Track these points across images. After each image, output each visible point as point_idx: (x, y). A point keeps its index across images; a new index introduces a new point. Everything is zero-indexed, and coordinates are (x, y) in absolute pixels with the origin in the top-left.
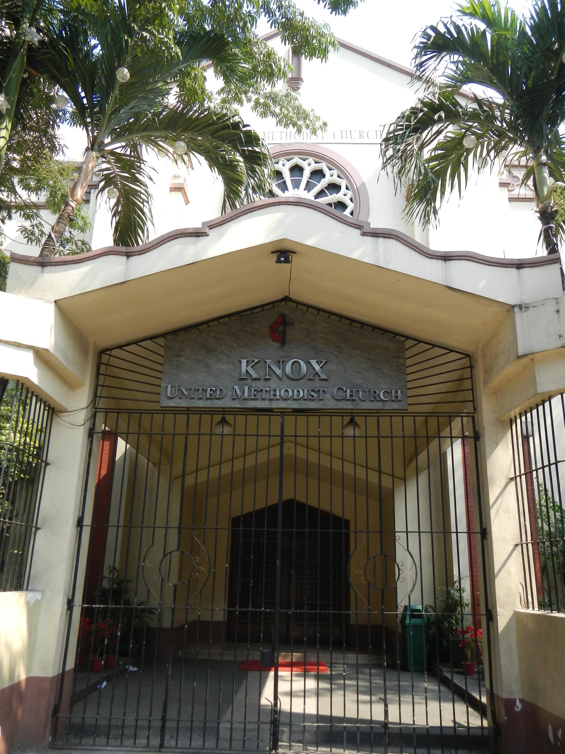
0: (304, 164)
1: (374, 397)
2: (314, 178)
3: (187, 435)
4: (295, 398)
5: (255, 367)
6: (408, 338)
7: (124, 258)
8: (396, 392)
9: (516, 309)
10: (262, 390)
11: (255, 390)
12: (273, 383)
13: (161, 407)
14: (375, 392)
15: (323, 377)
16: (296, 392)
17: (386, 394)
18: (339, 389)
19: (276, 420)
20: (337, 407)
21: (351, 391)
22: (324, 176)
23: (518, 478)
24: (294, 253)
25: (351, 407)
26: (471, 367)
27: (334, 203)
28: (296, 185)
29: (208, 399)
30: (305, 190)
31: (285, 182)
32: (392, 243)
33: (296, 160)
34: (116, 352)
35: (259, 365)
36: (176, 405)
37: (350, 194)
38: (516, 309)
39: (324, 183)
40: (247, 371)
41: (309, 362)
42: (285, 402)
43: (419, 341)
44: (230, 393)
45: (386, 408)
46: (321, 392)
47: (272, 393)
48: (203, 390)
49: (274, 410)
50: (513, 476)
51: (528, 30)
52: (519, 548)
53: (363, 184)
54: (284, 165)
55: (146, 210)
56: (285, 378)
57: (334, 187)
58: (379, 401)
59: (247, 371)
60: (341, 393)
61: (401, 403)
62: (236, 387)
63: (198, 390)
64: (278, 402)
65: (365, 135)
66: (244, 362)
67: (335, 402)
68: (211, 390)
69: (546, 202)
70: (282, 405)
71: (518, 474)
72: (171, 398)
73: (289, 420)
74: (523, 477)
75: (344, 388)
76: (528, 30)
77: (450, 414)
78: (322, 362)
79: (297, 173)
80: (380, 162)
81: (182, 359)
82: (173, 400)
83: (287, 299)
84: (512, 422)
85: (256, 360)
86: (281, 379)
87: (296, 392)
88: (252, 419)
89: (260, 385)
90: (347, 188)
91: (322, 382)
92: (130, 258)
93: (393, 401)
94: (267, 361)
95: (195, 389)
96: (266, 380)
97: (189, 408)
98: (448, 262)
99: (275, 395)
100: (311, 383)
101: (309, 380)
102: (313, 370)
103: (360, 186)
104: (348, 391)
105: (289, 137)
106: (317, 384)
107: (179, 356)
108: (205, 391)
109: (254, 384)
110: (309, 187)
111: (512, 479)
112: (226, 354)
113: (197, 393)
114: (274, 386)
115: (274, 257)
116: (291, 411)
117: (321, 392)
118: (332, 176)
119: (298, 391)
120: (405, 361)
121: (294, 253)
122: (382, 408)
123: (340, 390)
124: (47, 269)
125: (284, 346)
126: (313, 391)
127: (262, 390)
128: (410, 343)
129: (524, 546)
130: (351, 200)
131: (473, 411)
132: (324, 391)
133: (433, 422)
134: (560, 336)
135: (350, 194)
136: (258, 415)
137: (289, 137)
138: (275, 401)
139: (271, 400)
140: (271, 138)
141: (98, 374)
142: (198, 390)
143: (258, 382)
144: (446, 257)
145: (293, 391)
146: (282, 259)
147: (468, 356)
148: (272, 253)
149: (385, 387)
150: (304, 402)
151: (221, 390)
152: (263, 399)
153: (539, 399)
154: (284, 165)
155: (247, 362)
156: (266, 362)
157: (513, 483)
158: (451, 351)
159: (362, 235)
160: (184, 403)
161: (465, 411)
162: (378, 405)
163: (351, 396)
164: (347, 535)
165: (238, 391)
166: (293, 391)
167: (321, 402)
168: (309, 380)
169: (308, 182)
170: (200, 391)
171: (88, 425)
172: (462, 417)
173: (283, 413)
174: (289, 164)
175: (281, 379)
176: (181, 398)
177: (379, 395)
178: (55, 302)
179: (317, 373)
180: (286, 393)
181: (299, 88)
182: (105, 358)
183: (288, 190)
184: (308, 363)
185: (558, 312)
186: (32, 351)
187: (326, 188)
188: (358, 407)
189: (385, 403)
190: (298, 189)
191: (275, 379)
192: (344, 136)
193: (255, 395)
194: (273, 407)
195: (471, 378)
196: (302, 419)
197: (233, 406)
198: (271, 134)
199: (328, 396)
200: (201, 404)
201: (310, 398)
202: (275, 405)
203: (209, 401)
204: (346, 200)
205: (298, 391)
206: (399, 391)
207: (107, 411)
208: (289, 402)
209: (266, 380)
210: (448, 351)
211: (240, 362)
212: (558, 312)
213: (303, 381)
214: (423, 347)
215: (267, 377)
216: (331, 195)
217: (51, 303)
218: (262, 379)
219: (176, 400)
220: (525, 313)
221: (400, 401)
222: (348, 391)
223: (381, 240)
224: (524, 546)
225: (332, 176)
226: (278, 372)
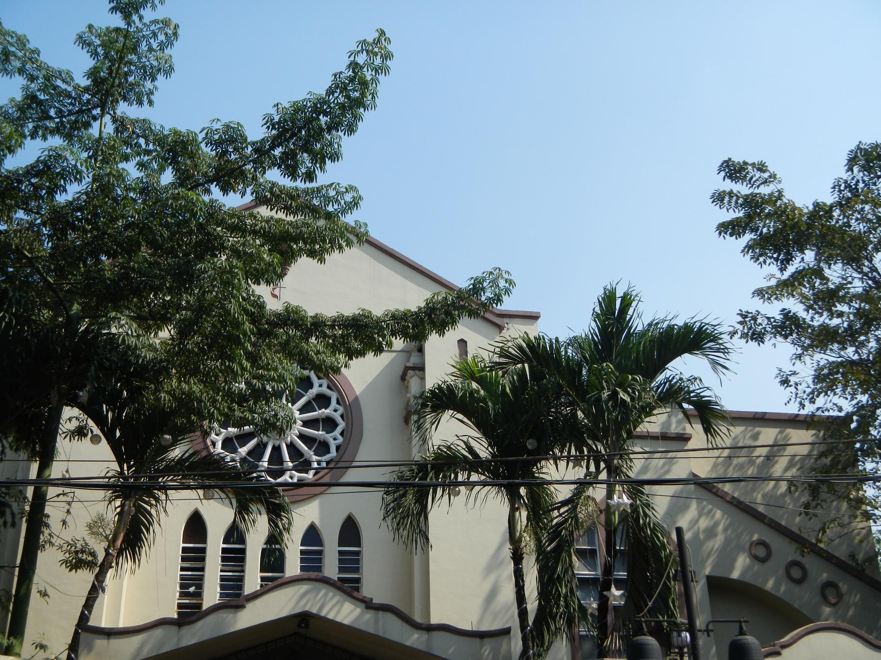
7: (176, 628)
22: (311, 385)
32: (390, 618)
37: (341, 410)
53: (356, 399)
55: (153, 512)
80: (381, 514)
90: (338, 403)
118: (320, 386)
130: (342, 416)
144: (430, 628)
146: (303, 625)
187: (313, 399)
204: (337, 416)
223: (381, 613)
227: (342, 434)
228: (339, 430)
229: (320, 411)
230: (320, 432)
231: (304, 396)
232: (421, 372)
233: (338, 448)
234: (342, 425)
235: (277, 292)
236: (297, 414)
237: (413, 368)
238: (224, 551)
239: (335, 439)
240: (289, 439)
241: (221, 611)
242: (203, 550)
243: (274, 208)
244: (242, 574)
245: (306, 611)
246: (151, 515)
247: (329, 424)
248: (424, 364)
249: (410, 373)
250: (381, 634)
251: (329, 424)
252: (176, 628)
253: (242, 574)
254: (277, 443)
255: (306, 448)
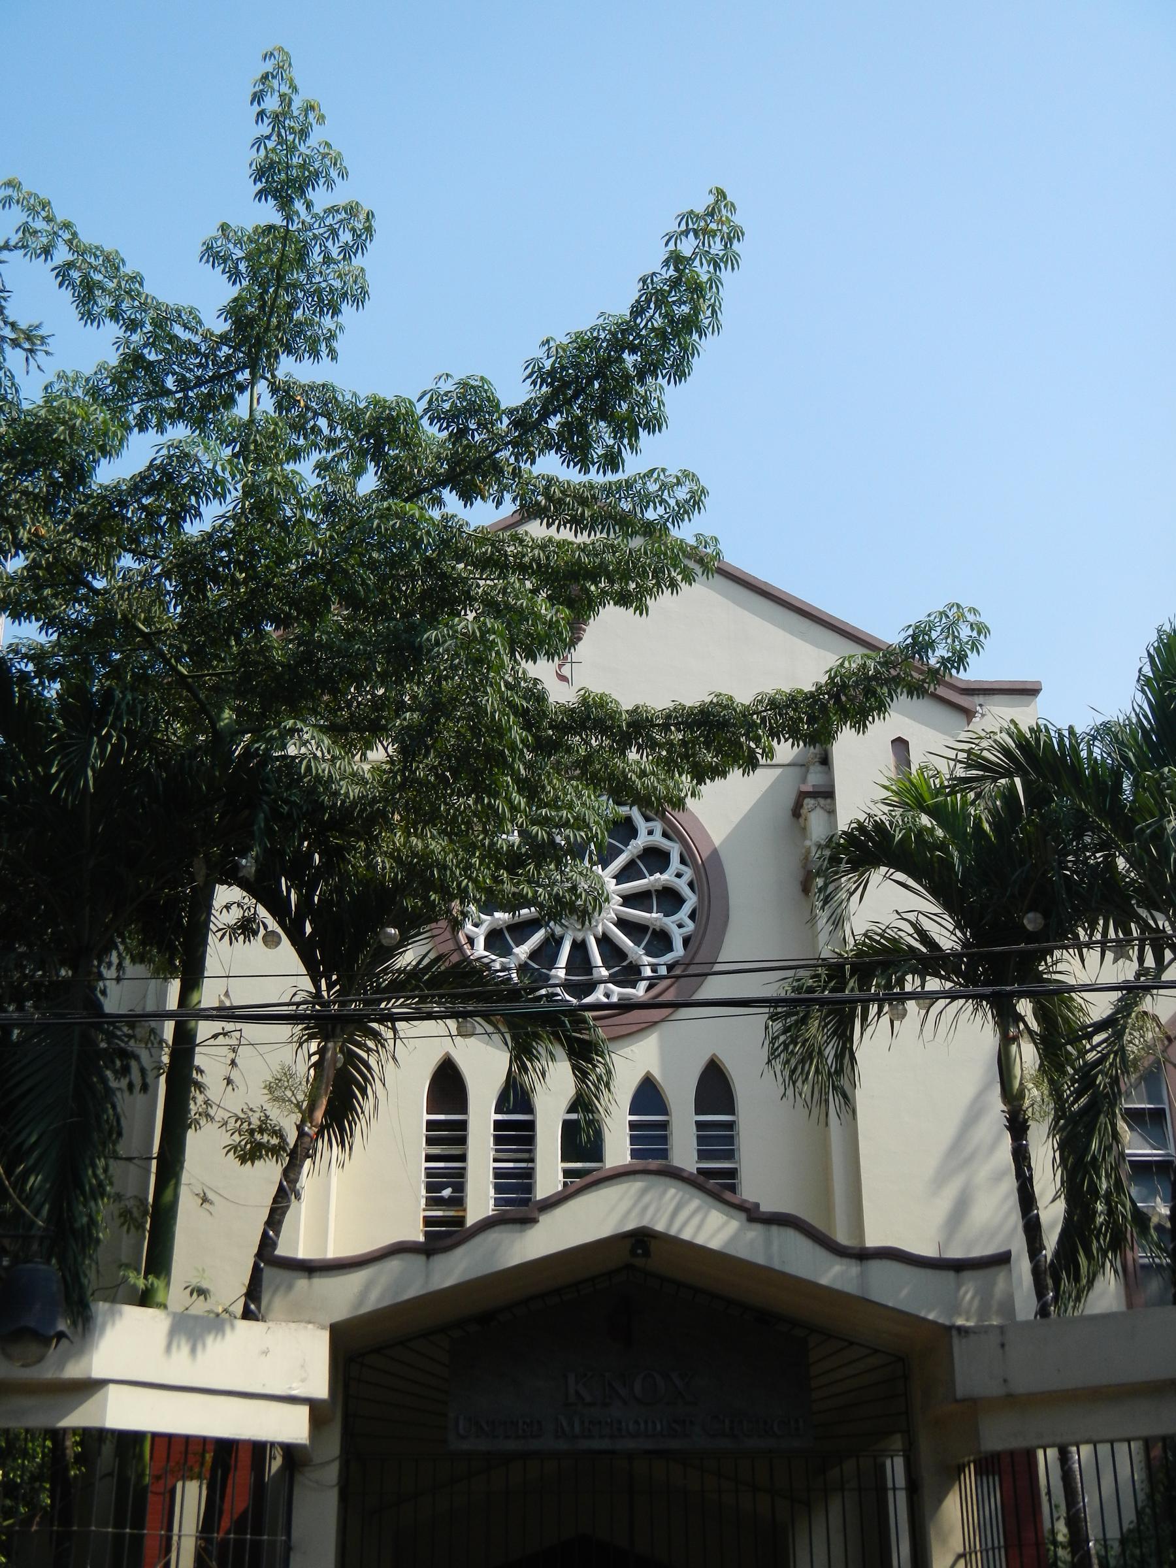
9: (954, 1333)
22: (634, 833)
32: (791, 1235)
37: (688, 873)
38: (954, 1333)
40: (577, 1393)
50: (961, 1550)
51: (986, 826)
53: (715, 853)
55: (372, 1062)
59: (577, 1393)
68: (524, 1423)
69: (1015, 1103)
70: (631, 1444)
76: (986, 826)
80: (764, 1054)
92: (431, 1258)
98: (865, 1262)
103: (708, 858)
118: (650, 833)
124: (315, 1274)
130: (691, 885)
134: (1005, 1381)
144: (863, 1255)
146: (640, 1251)
157: (962, 1561)
165: (565, 1424)
166: (646, 1422)
185: (1003, 1345)
187: (639, 857)
204: (682, 885)
212: (1003, 1345)
217: (323, 1328)
220: (964, 1341)
223: (774, 1229)
225: (650, 833)
227: (692, 916)
228: (687, 909)
229: (652, 878)
230: (654, 915)
231: (622, 851)
232: (829, 801)
233: (686, 941)
234: (691, 900)
235: (566, 671)
236: (611, 885)
237: (814, 795)
238: (498, 1125)
239: (680, 926)
240: (600, 929)
241: (497, 1229)
242: (463, 1125)
243: (553, 523)
244: (530, 1165)
245: (644, 1227)
246: (369, 1068)
247: (670, 899)
248: (833, 786)
249: (809, 803)
250: (777, 1265)
251: (670, 899)
252: (421, 1259)
253: (530, 1165)
254: (580, 936)
255: (631, 944)
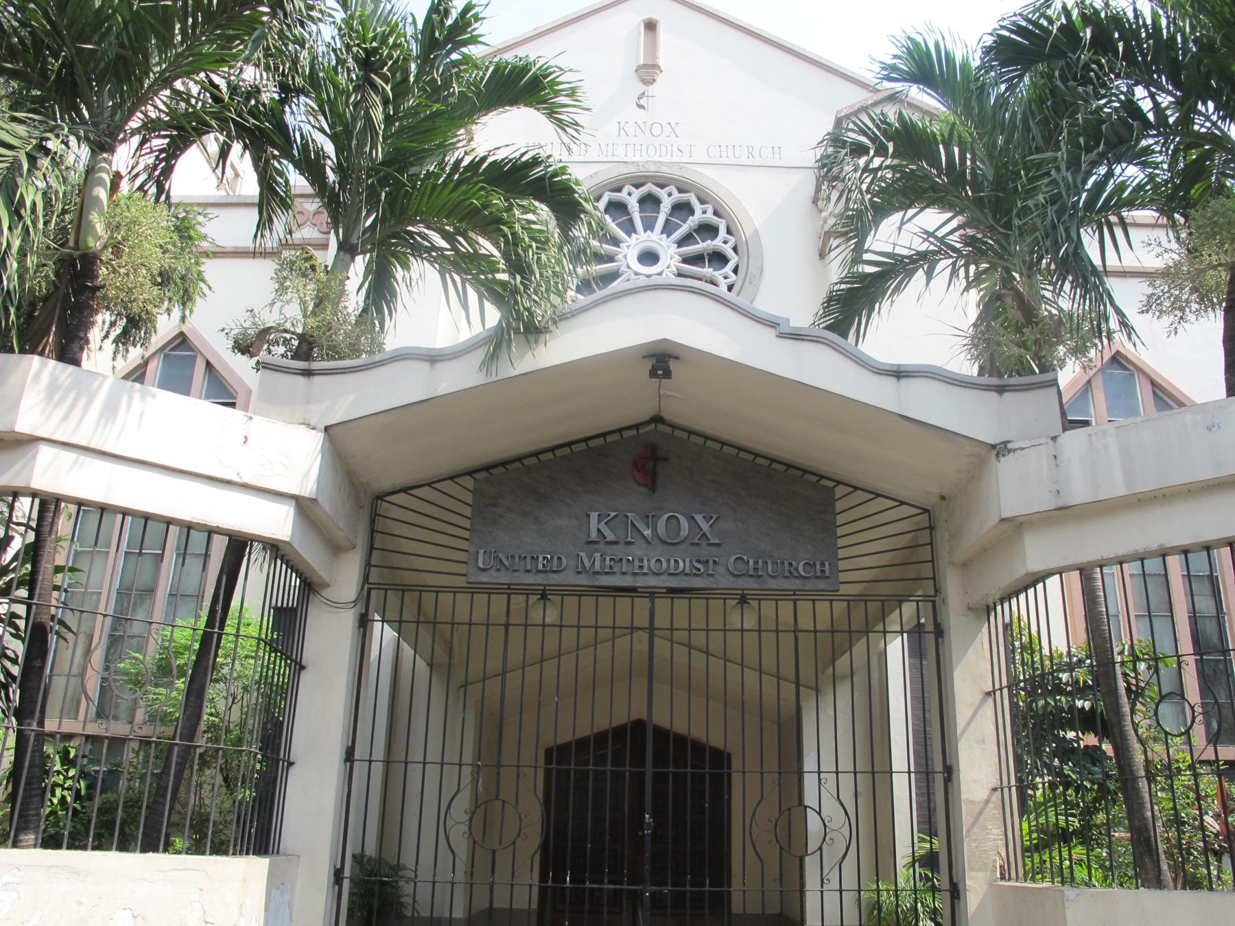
0: (662, 193)
1: (790, 572)
2: (676, 215)
3: (507, 626)
4: (672, 571)
5: (611, 523)
6: (839, 483)
8: (823, 564)
10: (621, 560)
11: (611, 559)
12: (637, 550)
13: (468, 583)
14: (791, 564)
15: (713, 541)
16: (672, 562)
17: (808, 568)
18: (737, 559)
19: (643, 604)
20: (734, 586)
21: (756, 563)
22: (692, 212)
23: (998, 693)
24: (677, 358)
25: (756, 586)
26: (931, 528)
27: (708, 254)
28: (649, 226)
29: (540, 571)
30: (662, 233)
31: (631, 220)
33: (649, 187)
34: (400, 498)
35: (617, 520)
36: (492, 580)
39: (693, 222)
40: (599, 530)
41: (693, 518)
42: (656, 578)
43: (856, 488)
44: (573, 563)
45: (807, 588)
46: (711, 564)
47: (637, 563)
48: (532, 557)
49: (639, 590)
50: (990, 689)
52: (999, 793)
54: (630, 194)
56: (656, 542)
57: (707, 230)
58: (796, 577)
59: (599, 530)
60: (741, 566)
61: (830, 581)
62: (583, 554)
63: (525, 557)
64: (646, 577)
65: (756, 154)
66: (594, 516)
67: (732, 579)
68: (544, 558)
70: (653, 581)
71: (997, 686)
72: (484, 570)
73: (662, 604)
74: (1005, 691)
75: (745, 558)
77: (899, 598)
78: (711, 518)
79: (649, 206)
81: (499, 510)
82: (487, 573)
83: (657, 419)
84: (989, 609)
85: (613, 514)
86: (649, 543)
87: (672, 562)
88: (606, 602)
89: (618, 551)
91: (712, 548)
93: (817, 578)
94: (629, 514)
95: (520, 557)
96: (628, 543)
97: (509, 585)
99: (641, 567)
100: (695, 550)
101: (693, 544)
102: (698, 530)
104: (751, 562)
105: (638, 154)
106: (705, 551)
107: (495, 505)
108: (534, 559)
109: (609, 549)
110: (668, 229)
111: (988, 694)
112: (567, 504)
113: (522, 563)
114: (639, 553)
115: (648, 365)
116: (665, 591)
117: (711, 564)
118: (704, 212)
119: (676, 561)
120: (835, 518)
121: (677, 358)
122: (801, 588)
123: (739, 561)
125: (654, 492)
126: (698, 561)
127: (621, 560)
128: (841, 491)
129: (1006, 790)
131: (933, 593)
132: (715, 562)
133: (873, 607)
135: (732, 240)
136: (615, 596)
137: (638, 154)
138: (642, 577)
139: (635, 574)
140: (610, 154)
141: (373, 531)
142: (525, 557)
143: (615, 547)
144: (899, 373)
145: (669, 561)
147: (926, 511)
148: (644, 357)
149: (806, 557)
150: (686, 578)
151: (559, 558)
152: (624, 574)
153: (1030, 579)
154: (630, 194)
155: (599, 515)
156: (627, 516)
158: (902, 503)
159: (778, 336)
160: (503, 578)
161: (920, 593)
162: (796, 584)
163: (756, 569)
164: (729, 776)
166: (669, 561)
167: (711, 579)
168: (693, 544)
169: (667, 221)
170: (529, 559)
171: (360, 608)
172: (917, 602)
173: (652, 594)
174: (638, 193)
175: (649, 543)
176: (498, 570)
177: (797, 569)
178: (326, 429)
179: (704, 534)
180: (658, 565)
181: (654, 80)
182: (384, 507)
183: (636, 233)
184: (691, 519)
186: (293, 502)
187: (695, 231)
188: (765, 587)
189: (806, 581)
190: (652, 231)
191: (642, 543)
192: (724, 154)
193: (611, 567)
194: (639, 584)
195: (931, 544)
196: (681, 604)
197: (577, 583)
198: (610, 147)
199: (720, 569)
200: (530, 579)
201: (695, 571)
202: (640, 582)
203: (542, 575)
204: (728, 250)
205: (676, 561)
206: (827, 564)
207: (379, 586)
208: (662, 578)
209: (628, 543)
210: (897, 504)
211: (589, 516)
213: (683, 546)
214: (860, 496)
215: (629, 539)
216: (703, 241)
218: (622, 542)
219: (492, 572)
221: (828, 578)
222: (751, 562)
224: (1006, 790)
225: (704, 212)
226: (647, 533)
227: (735, 271)
228: (731, 265)
235: (643, 102)
239: (726, 278)
247: (719, 258)
252: (427, 365)
